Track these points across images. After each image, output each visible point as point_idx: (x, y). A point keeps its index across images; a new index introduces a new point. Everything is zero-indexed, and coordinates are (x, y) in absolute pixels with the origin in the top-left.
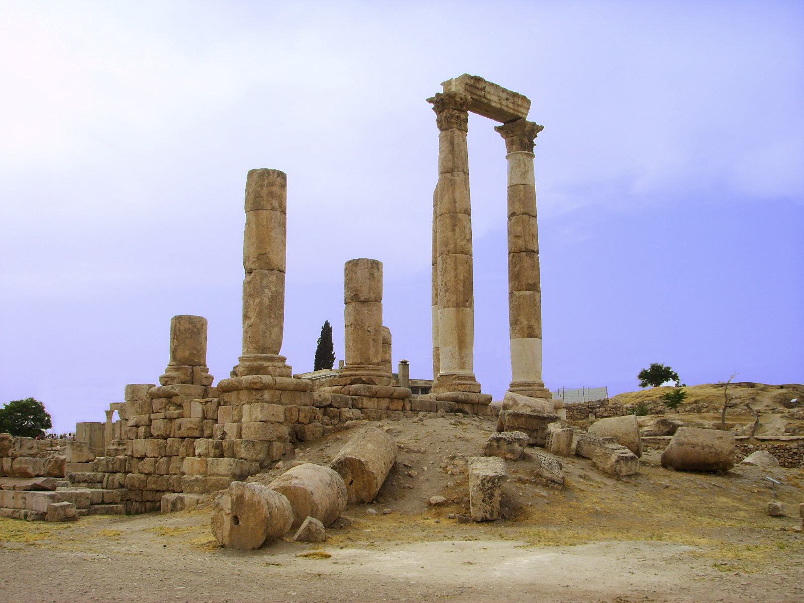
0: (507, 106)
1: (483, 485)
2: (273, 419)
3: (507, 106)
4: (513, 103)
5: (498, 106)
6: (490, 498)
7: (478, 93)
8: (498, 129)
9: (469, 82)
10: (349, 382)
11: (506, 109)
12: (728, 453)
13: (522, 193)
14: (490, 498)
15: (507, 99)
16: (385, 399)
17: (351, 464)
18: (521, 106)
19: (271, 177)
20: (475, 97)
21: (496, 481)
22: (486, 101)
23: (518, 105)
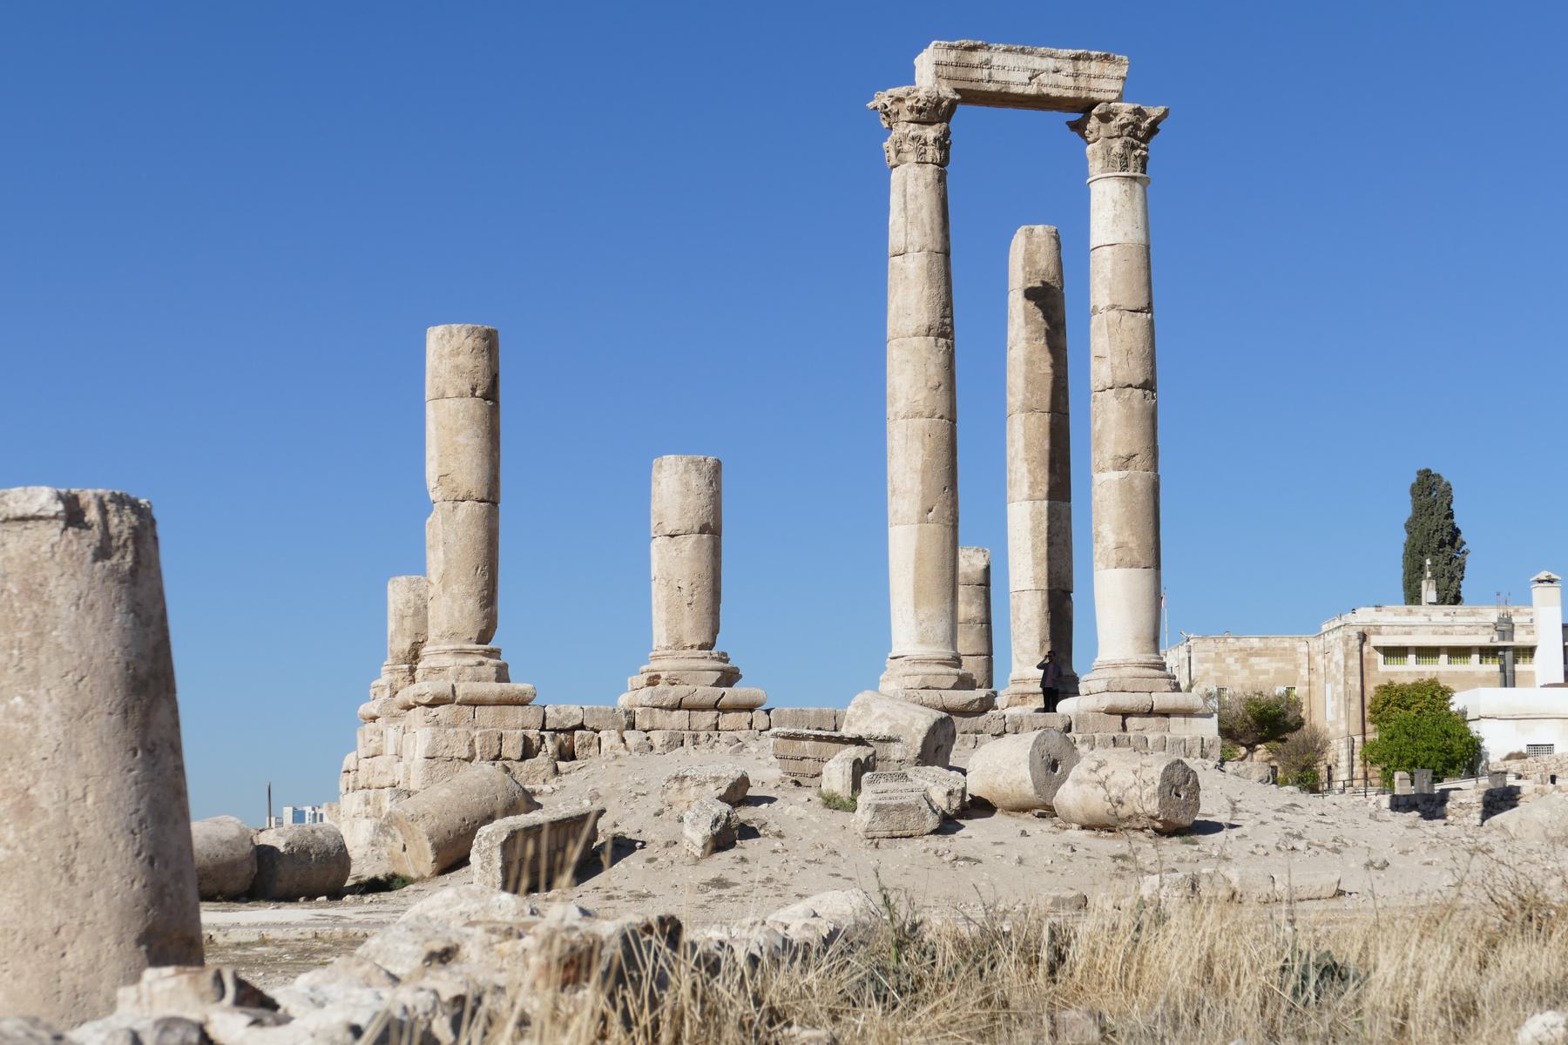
2: (448, 753)
4: (1076, 76)
5: (1032, 90)
9: (943, 58)
11: (1054, 92)
13: (1108, 265)
20: (961, 85)
22: (993, 87)
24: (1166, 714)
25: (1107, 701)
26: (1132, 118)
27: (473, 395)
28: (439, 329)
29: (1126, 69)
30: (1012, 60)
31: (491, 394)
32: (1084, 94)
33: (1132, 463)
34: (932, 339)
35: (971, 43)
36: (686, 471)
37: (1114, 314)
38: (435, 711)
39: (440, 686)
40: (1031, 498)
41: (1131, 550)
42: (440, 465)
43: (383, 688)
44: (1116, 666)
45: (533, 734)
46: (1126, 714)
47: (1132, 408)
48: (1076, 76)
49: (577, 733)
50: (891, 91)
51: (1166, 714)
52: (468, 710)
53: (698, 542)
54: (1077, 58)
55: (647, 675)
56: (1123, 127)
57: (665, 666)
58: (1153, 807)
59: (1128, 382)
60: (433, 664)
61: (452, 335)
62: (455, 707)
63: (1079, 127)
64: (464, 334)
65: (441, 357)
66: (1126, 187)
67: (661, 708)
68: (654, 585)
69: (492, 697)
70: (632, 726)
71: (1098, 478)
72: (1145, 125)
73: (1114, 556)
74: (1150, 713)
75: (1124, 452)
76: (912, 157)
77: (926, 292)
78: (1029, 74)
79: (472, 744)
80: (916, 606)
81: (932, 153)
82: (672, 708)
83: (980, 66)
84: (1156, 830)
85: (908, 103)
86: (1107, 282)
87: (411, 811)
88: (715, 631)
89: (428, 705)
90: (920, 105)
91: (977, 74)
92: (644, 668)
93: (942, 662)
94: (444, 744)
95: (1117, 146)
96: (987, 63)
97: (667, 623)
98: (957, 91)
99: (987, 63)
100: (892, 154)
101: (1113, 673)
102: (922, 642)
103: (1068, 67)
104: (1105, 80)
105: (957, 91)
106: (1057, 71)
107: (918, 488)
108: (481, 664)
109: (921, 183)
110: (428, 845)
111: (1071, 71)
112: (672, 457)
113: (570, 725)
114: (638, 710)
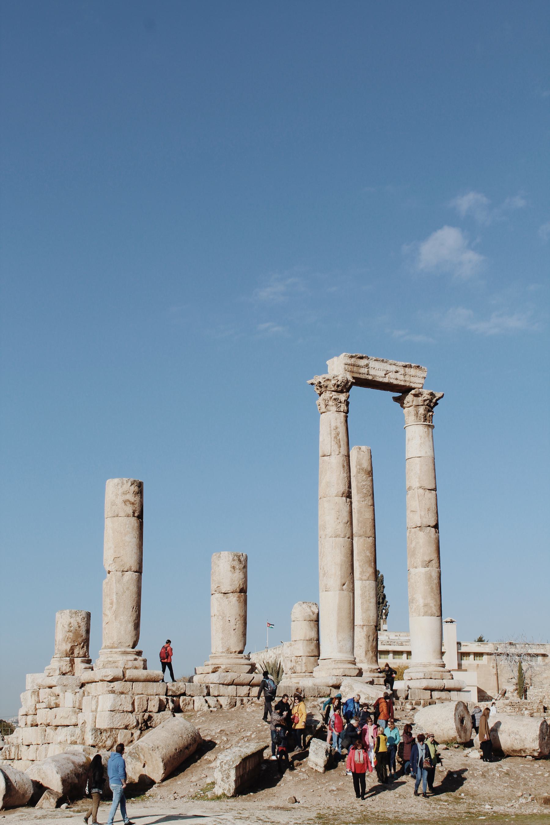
0: (397, 379)
1: (222, 767)
2: (121, 708)
4: (405, 375)
5: (386, 380)
6: (227, 778)
8: (396, 399)
10: (210, 670)
11: (395, 382)
12: (531, 740)
14: (227, 778)
15: (397, 372)
16: (245, 687)
17: (142, 749)
19: (125, 486)
21: (231, 763)
22: (370, 378)
24: (449, 690)
25: (425, 683)
26: (429, 397)
27: (134, 516)
28: (116, 480)
30: (377, 365)
31: (140, 517)
32: (408, 384)
33: (430, 564)
34: (344, 498)
36: (233, 560)
37: (421, 491)
38: (112, 684)
39: (111, 673)
40: (361, 580)
41: (431, 607)
42: (115, 552)
43: (55, 670)
44: (425, 666)
45: (163, 698)
47: (430, 536)
49: (182, 698)
50: (324, 376)
51: (449, 690)
52: (129, 683)
53: (239, 597)
54: (405, 366)
55: (213, 667)
56: (425, 401)
57: (224, 662)
58: (536, 745)
59: (428, 524)
60: (110, 659)
61: (123, 484)
62: (123, 683)
63: (400, 400)
64: (130, 484)
65: (117, 495)
66: (426, 430)
67: (223, 684)
68: (214, 620)
69: (142, 678)
70: (208, 694)
71: (413, 571)
72: (434, 401)
73: (422, 610)
74: (443, 690)
75: (427, 559)
76: (334, 409)
77: (342, 475)
78: (385, 372)
79: (133, 704)
80: (338, 632)
81: (343, 407)
82: (228, 685)
84: (533, 757)
85: (333, 382)
86: (416, 474)
87: (151, 745)
88: (245, 644)
89: (109, 681)
90: (339, 383)
91: (364, 370)
92: (210, 662)
94: (120, 703)
95: (422, 410)
96: (367, 365)
97: (222, 639)
99: (367, 365)
100: (323, 406)
101: (425, 670)
102: (340, 652)
103: (402, 371)
105: (354, 378)
106: (397, 372)
107: (338, 573)
108: (136, 659)
109: (338, 421)
110: (161, 765)
111: (403, 372)
112: (226, 552)
113: (179, 693)
114: (211, 685)
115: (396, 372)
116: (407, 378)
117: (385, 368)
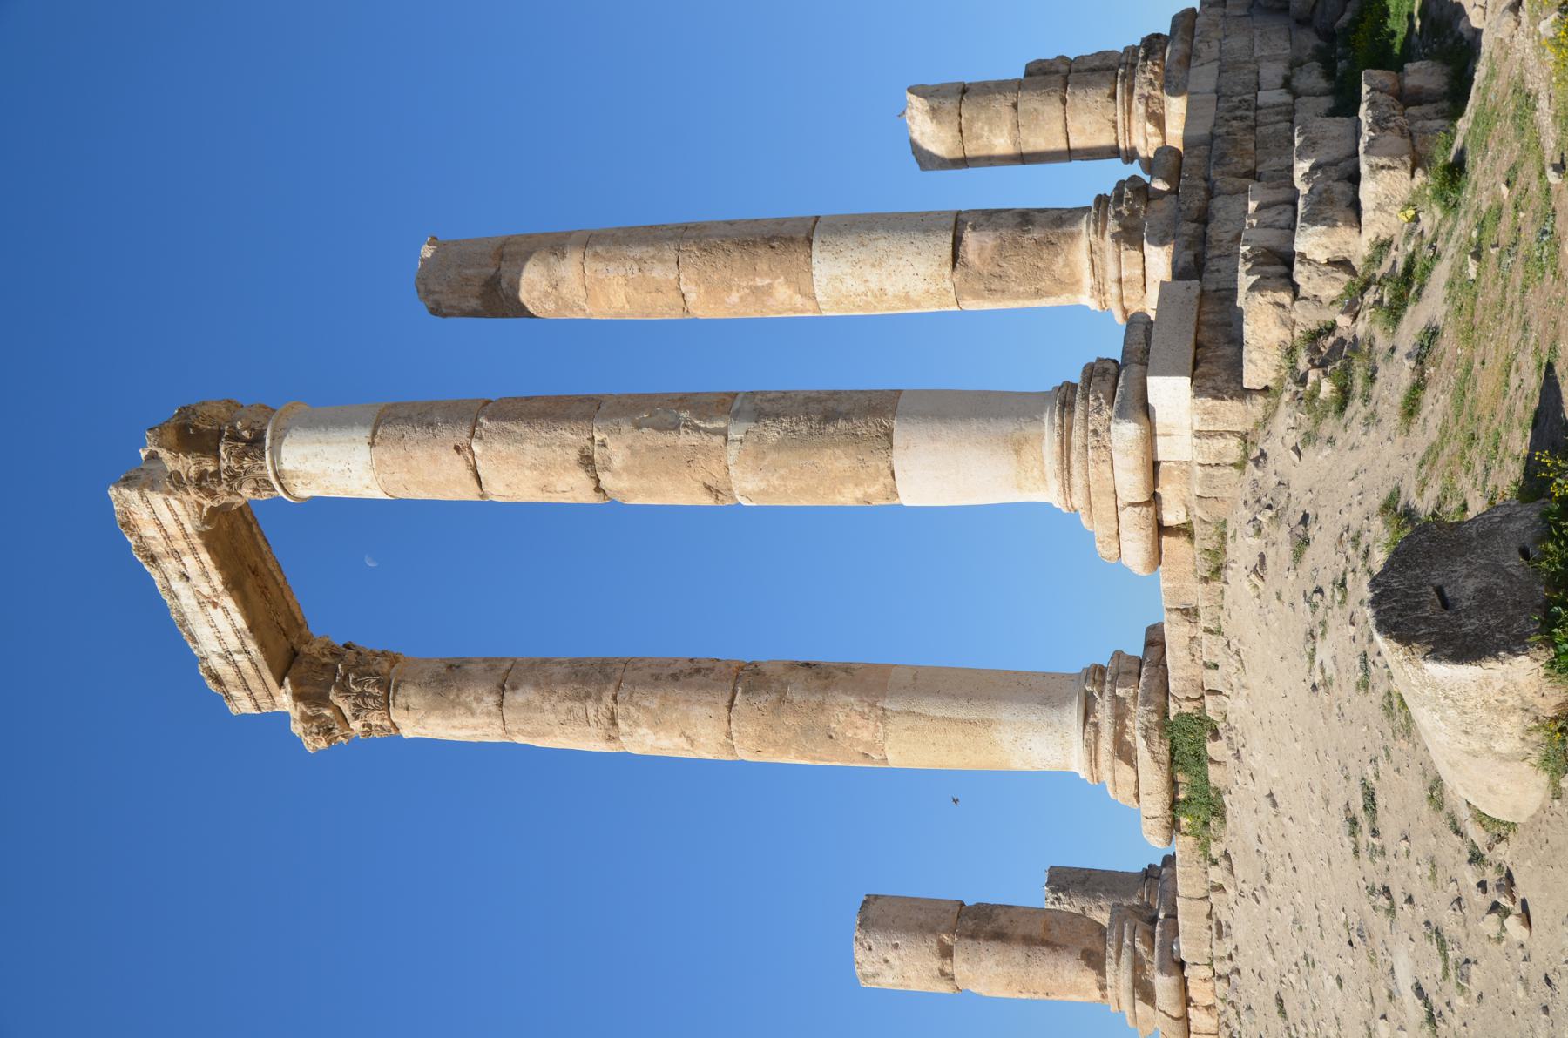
0: (205, 574)
3: (205, 574)
7: (251, 671)
11: (217, 578)
15: (185, 577)
18: (160, 525)
22: (252, 647)
23: (167, 537)
29: (126, 492)
30: (203, 631)
32: (197, 541)
35: (209, 682)
46: (1161, 529)
48: (178, 555)
54: (153, 559)
74: (1154, 500)
78: (210, 608)
83: (234, 664)
93: (1094, 762)
96: (226, 656)
98: (281, 685)
103: (170, 565)
104: (161, 519)
105: (281, 685)
106: (185, 577)
115: (188, 578)
116: (181, 545)
117: (197, 608)
